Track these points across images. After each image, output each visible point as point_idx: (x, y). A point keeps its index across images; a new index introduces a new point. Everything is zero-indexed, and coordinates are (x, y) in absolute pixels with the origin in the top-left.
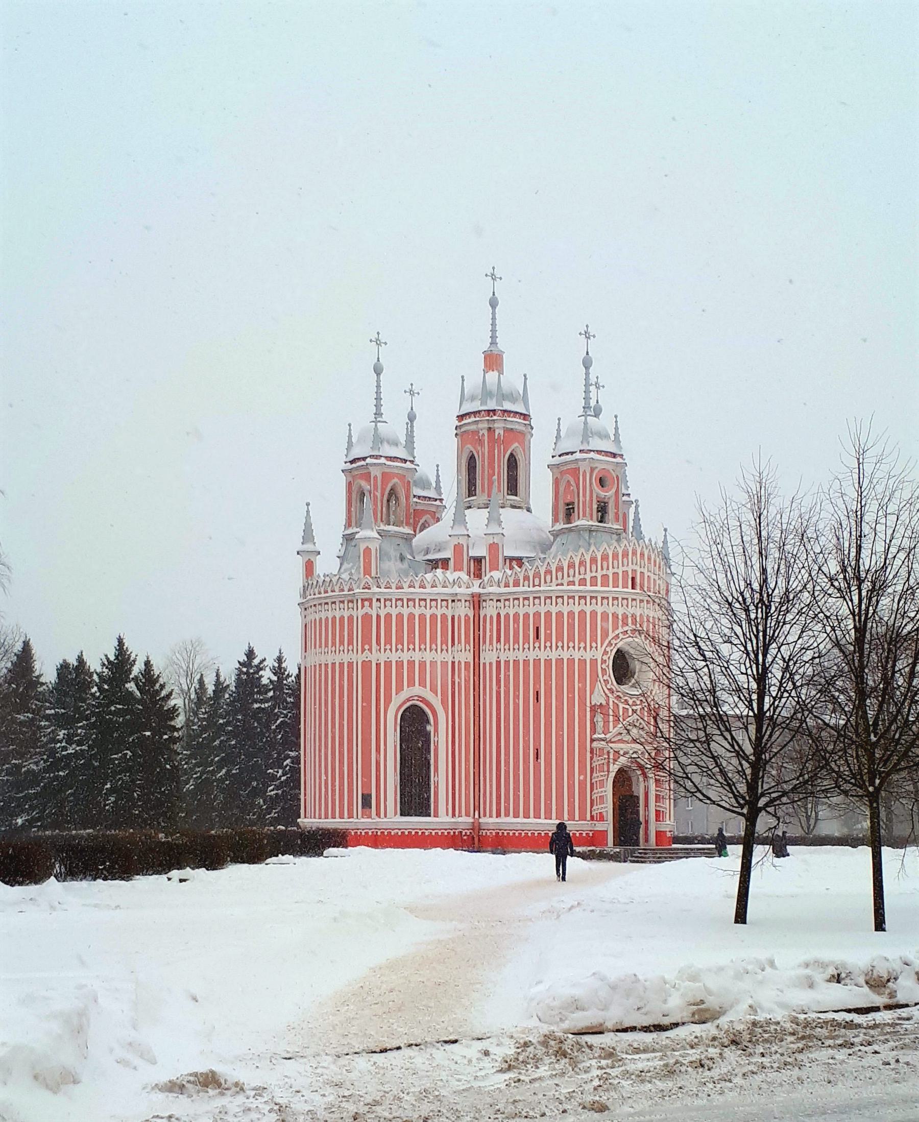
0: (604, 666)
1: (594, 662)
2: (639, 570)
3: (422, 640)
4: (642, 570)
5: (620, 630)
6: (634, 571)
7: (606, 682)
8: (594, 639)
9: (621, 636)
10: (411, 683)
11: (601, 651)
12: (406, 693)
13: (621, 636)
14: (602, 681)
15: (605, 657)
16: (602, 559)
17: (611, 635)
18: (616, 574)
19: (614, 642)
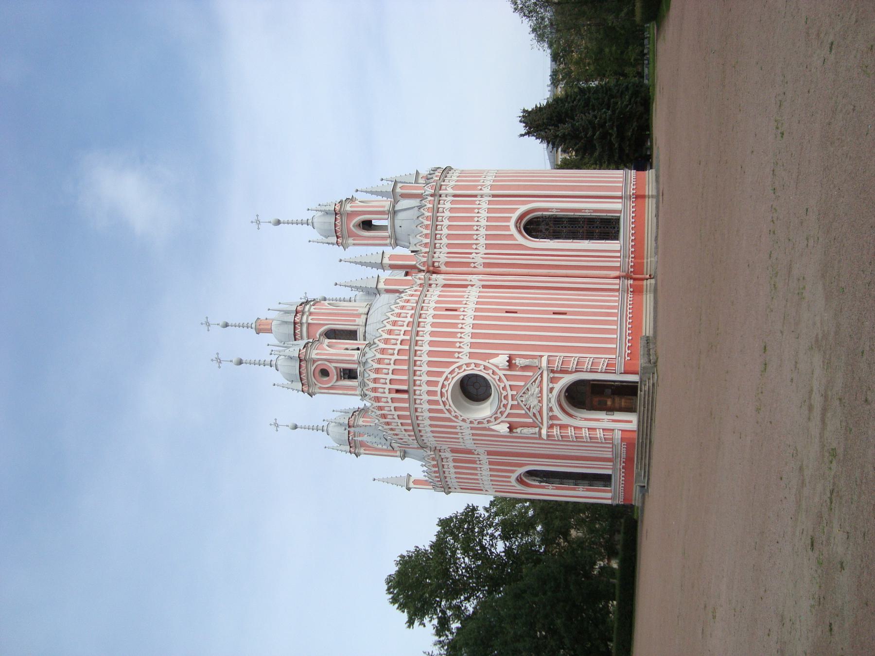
0: (476, 422)
1: (472, 428)
2: (388, 386)
3: (476, 474)
4: (388, 381)
5: (441, 407)
6: (390, 391)
7: (488, 422)
8: (455, 427)
9: (447, 407)
10: (510, 482)
11: (462, 424)
12: (514, 483)
13: (447, 407)
14: (488, 425)
15: (468, 421)
16: (385, 418)
17: (447, 415)
18: (396, 409)
19: (453, 413)
